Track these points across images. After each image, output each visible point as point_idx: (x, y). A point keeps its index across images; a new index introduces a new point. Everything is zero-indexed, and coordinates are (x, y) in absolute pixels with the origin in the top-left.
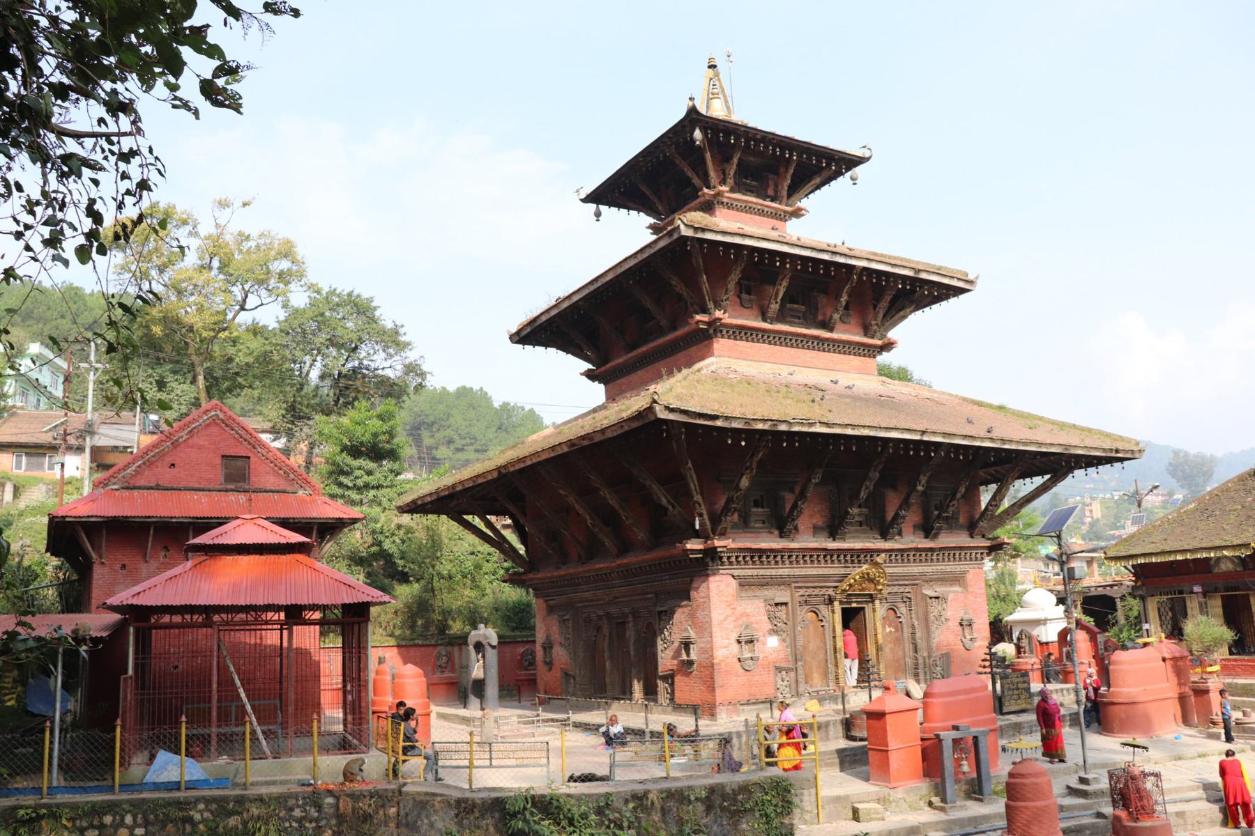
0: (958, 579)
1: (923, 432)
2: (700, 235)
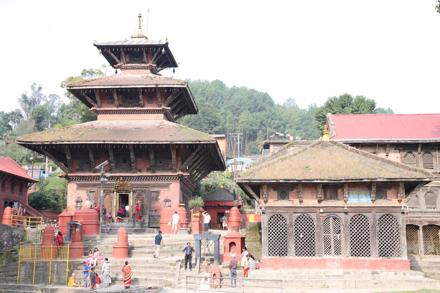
0: (167, 186)
1: (104, 141)
2: (72, 88)
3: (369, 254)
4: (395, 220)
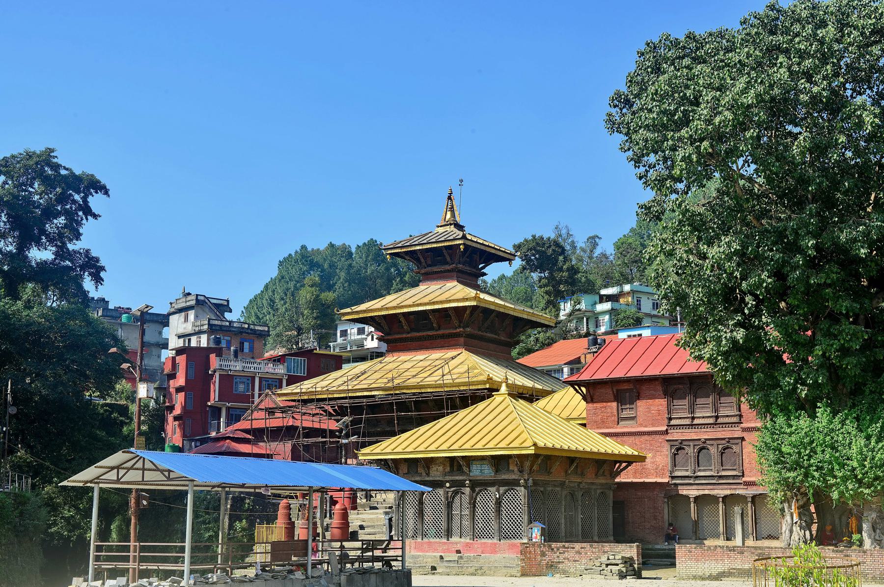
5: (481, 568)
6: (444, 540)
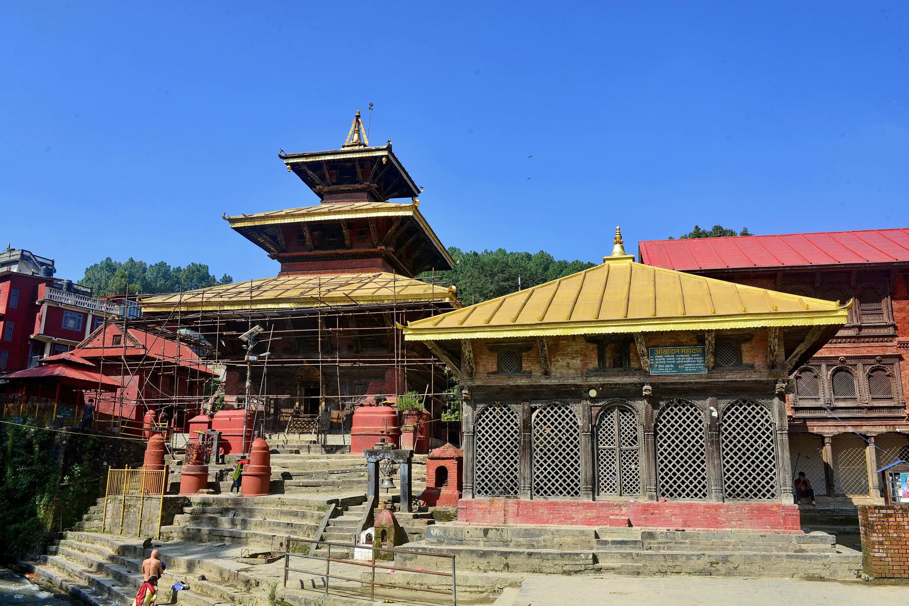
3: (704, 491)
4: (762, 413)
5: (725, 559)
6: (585, 499)
